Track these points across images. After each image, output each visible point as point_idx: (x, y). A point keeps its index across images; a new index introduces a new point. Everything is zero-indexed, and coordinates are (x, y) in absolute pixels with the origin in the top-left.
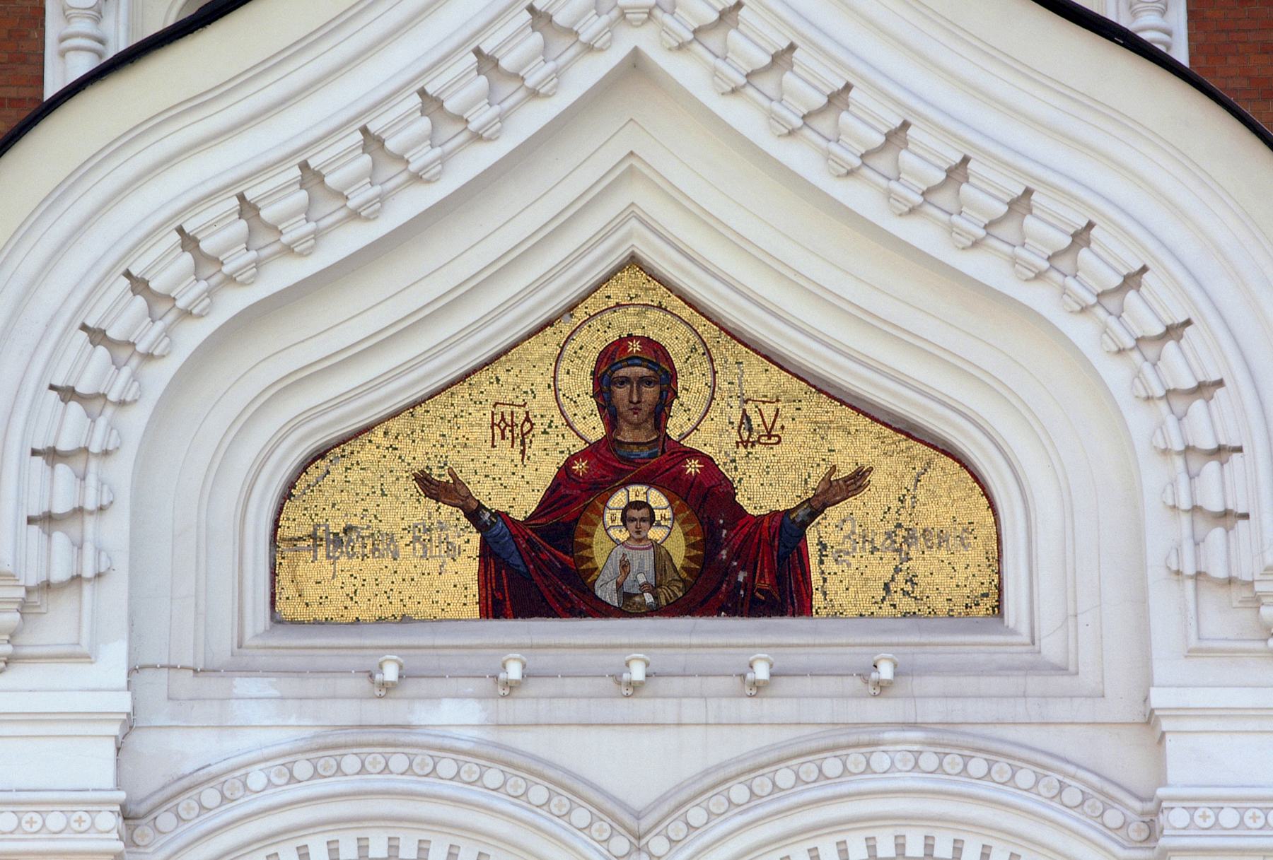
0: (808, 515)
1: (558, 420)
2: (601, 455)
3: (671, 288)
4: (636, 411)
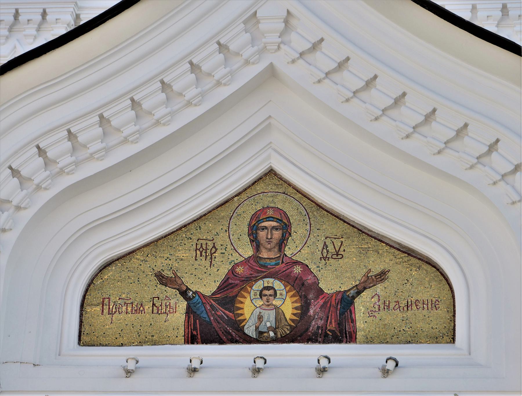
0: (356, 293)
1: (229, 247)
2: (250, 264)
3: (290, 184)
4: (269, 243)
